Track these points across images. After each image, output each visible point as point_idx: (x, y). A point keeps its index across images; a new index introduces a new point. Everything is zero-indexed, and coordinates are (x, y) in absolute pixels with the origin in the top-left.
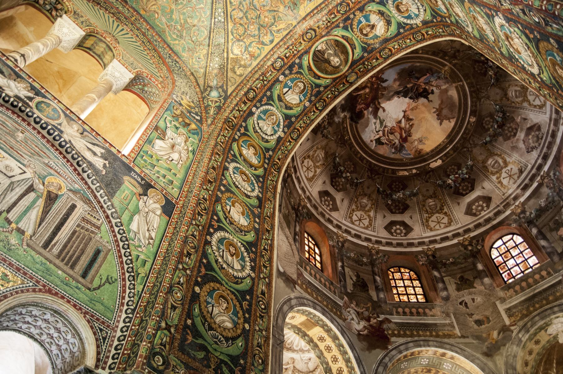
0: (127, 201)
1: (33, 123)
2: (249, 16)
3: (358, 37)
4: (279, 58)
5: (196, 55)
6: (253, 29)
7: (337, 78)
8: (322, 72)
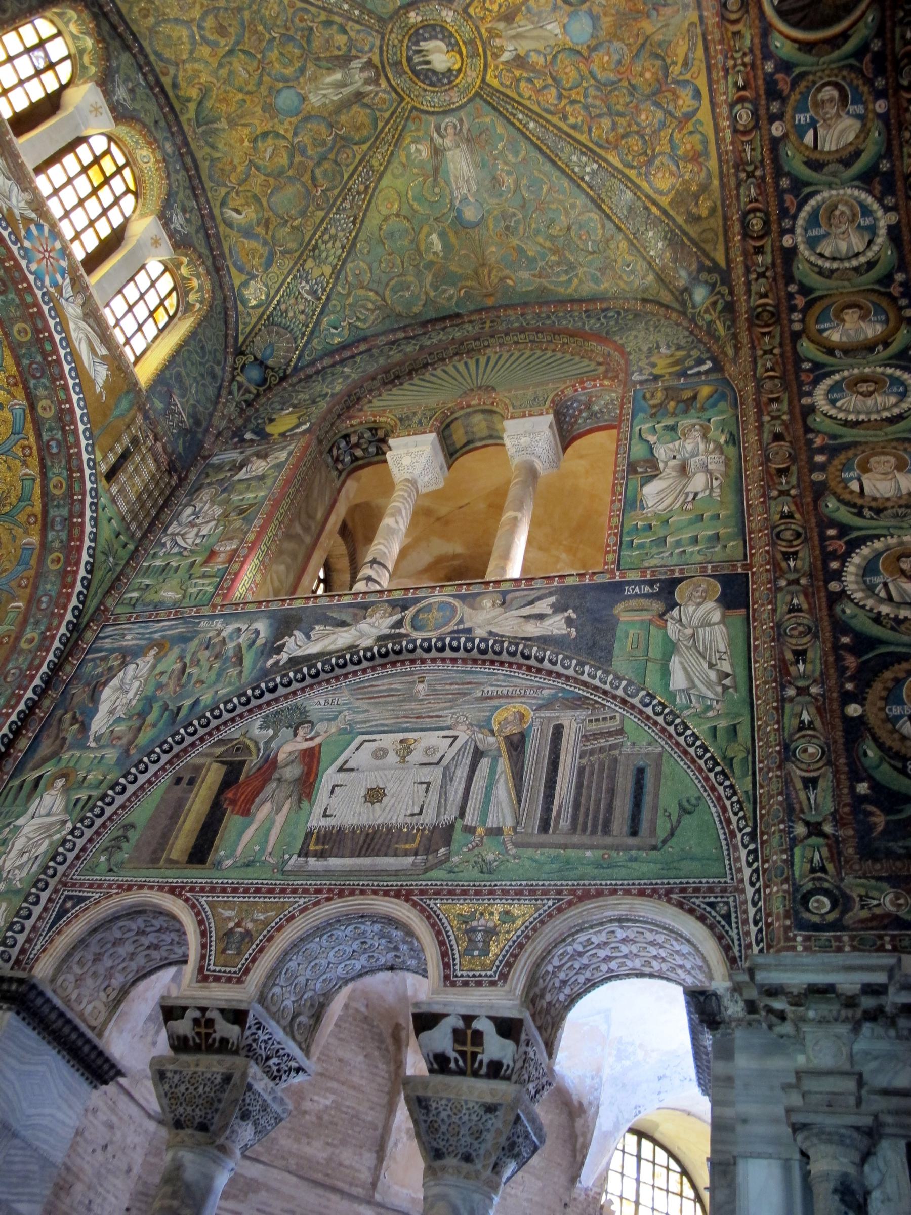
0: (642, 646)
1: (425, 655)
2: (619, 107)
4: (732, 106)
6: (649, 116)
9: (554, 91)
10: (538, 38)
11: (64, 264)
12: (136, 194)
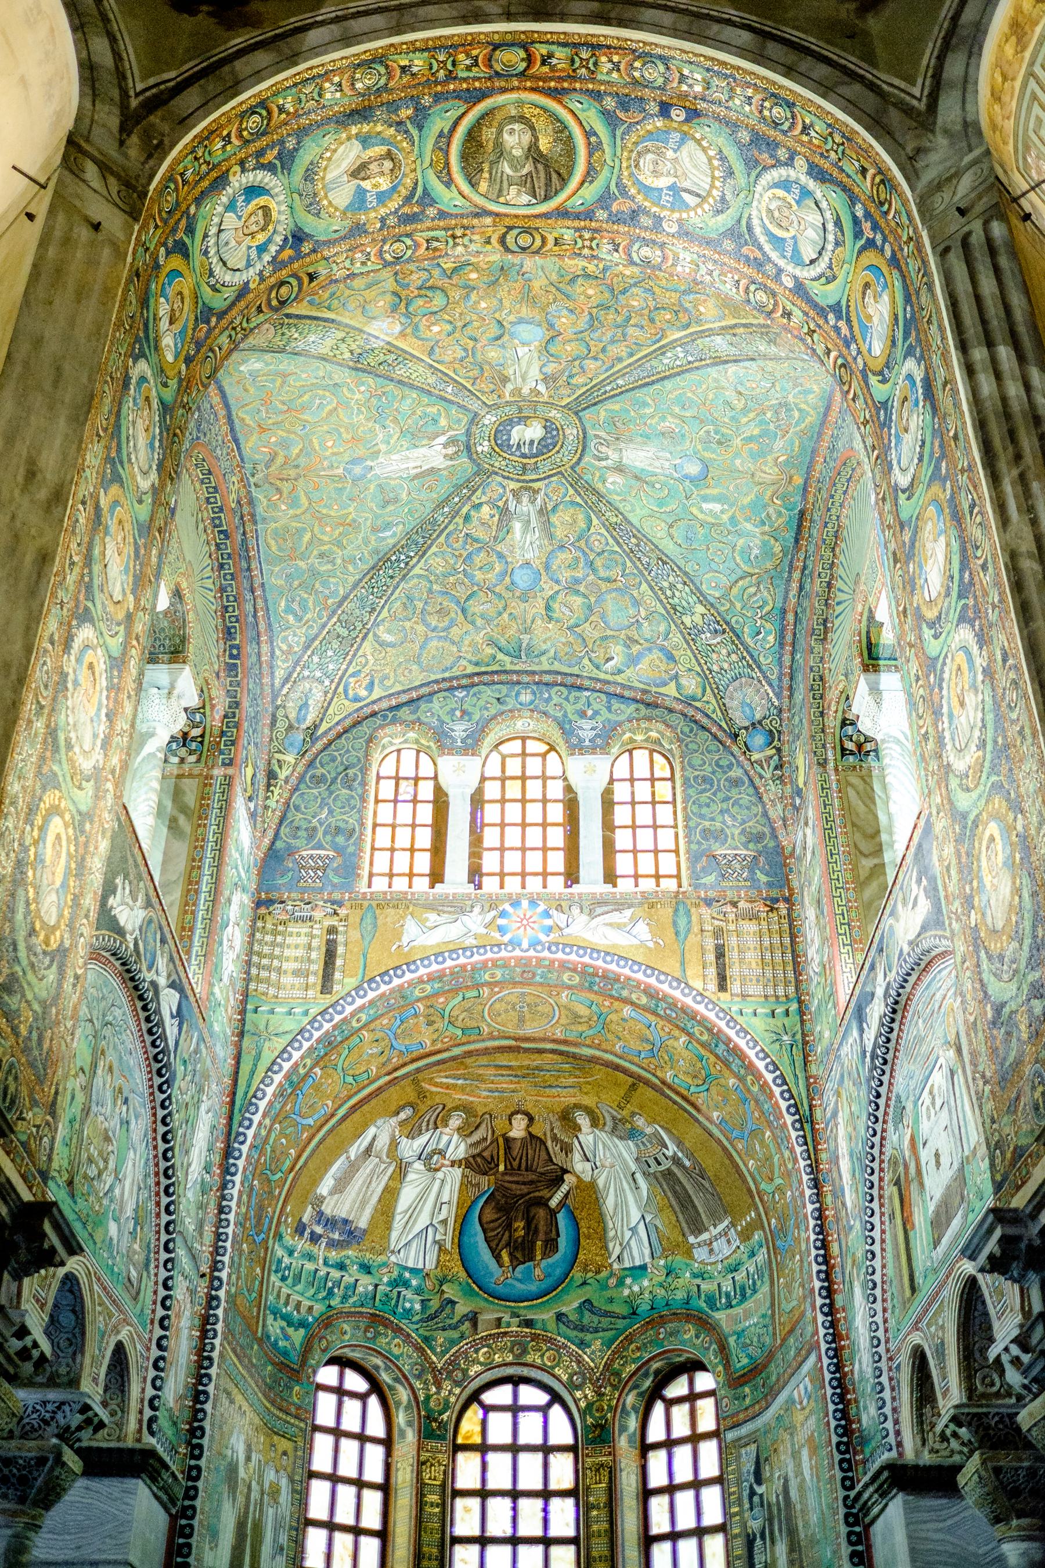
8: (570, 137)
10: (529, 363)
11: (542, 907)
12: (552, 748)
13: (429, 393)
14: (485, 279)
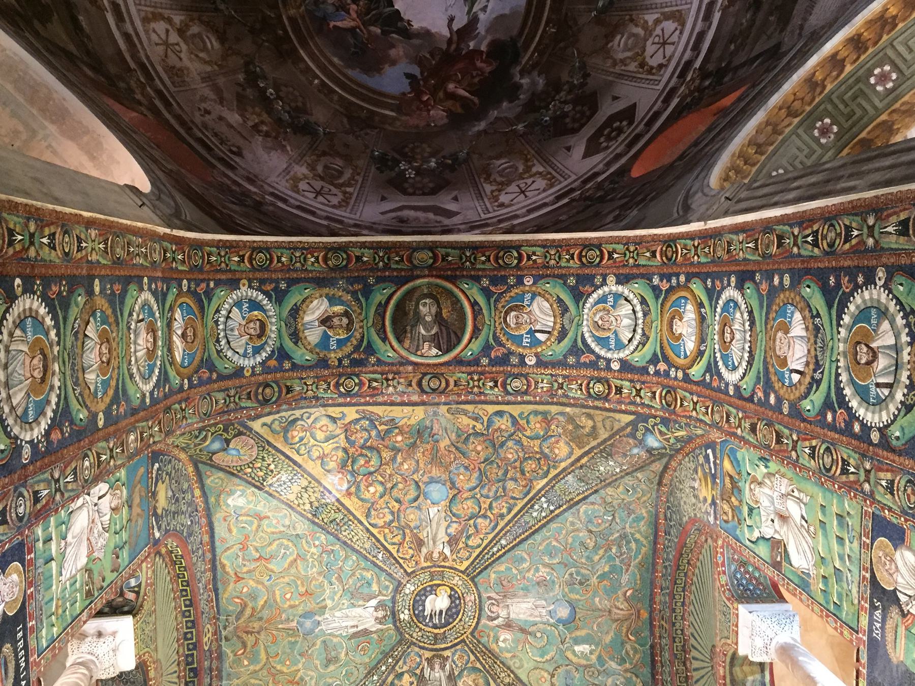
3: (362, 321)
4: (508, 393)
5: (628, 499)
7: (447, 278)
8: (462, 308)
9: (479, 520)
10: (438, 524)
13: (366, 558)
14: (408, 442)
